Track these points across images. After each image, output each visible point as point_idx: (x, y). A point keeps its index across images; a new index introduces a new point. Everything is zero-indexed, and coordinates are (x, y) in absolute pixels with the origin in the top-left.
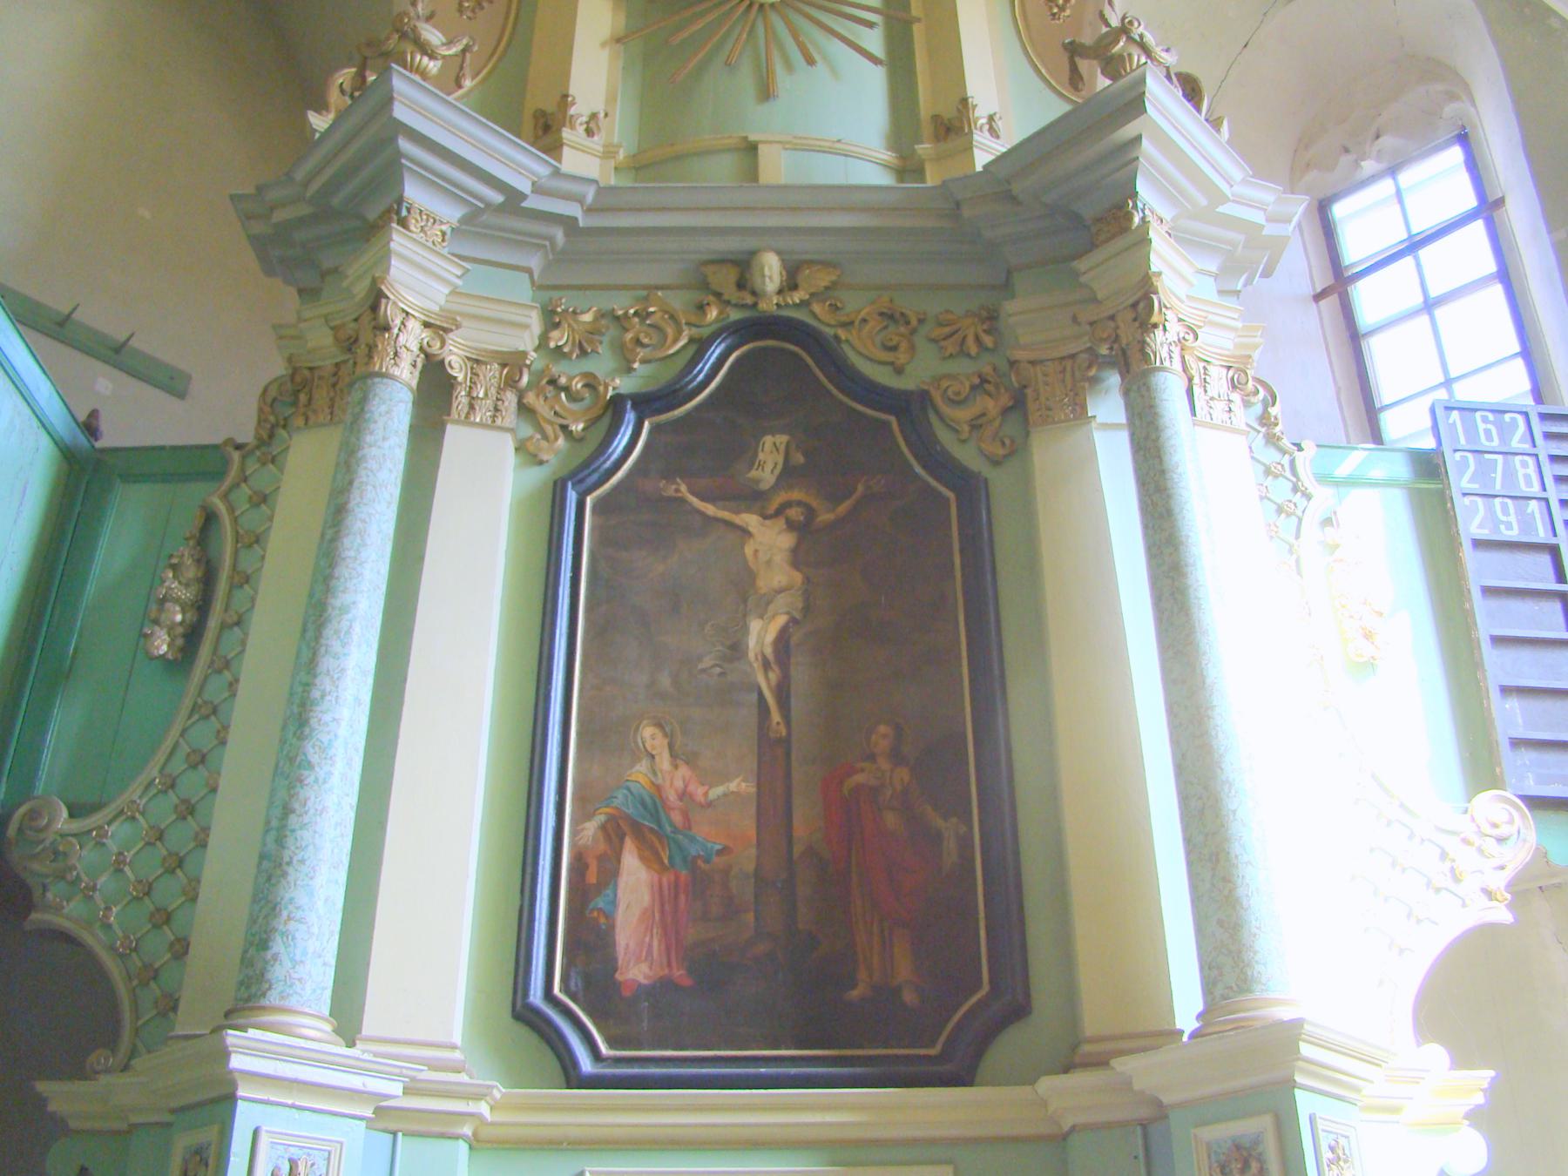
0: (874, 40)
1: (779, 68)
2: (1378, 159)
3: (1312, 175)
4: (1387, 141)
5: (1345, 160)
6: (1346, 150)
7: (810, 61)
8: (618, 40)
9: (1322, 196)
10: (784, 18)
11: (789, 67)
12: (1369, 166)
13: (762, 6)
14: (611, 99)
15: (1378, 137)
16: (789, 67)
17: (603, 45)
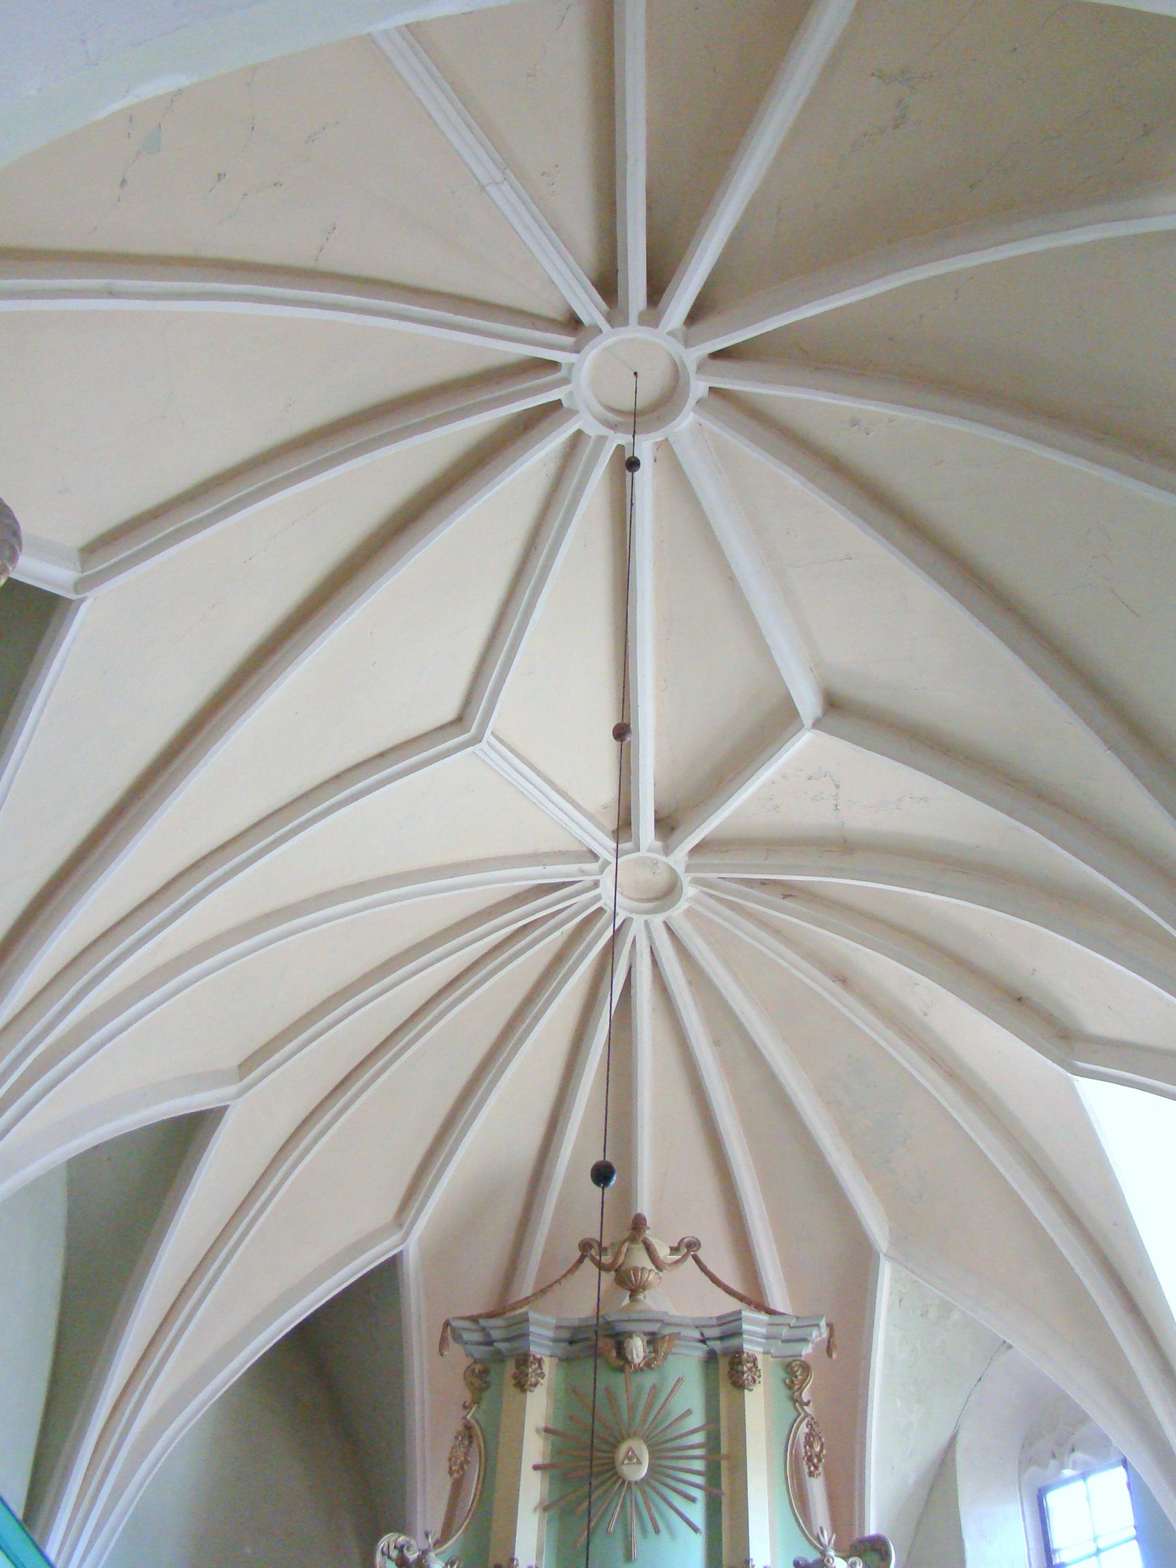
0: (697, 1513)
1: (637, 1534)
2: (1074, 1468)
3: (1033, 1469)
4: (1079, 1455)
5: (1053, 1463)
6: (1054, 1456)
7: (657, 1530)
8: (545, 1509)
9: (1040, 1486)
10: (643, 1492)
11: (644, 1532)
12: (1067, 1473)
13: (629, 1483)
14: (539, 1555)
15: (1073, 1450)
16: (644, 1532)
17: (535, 1510)
